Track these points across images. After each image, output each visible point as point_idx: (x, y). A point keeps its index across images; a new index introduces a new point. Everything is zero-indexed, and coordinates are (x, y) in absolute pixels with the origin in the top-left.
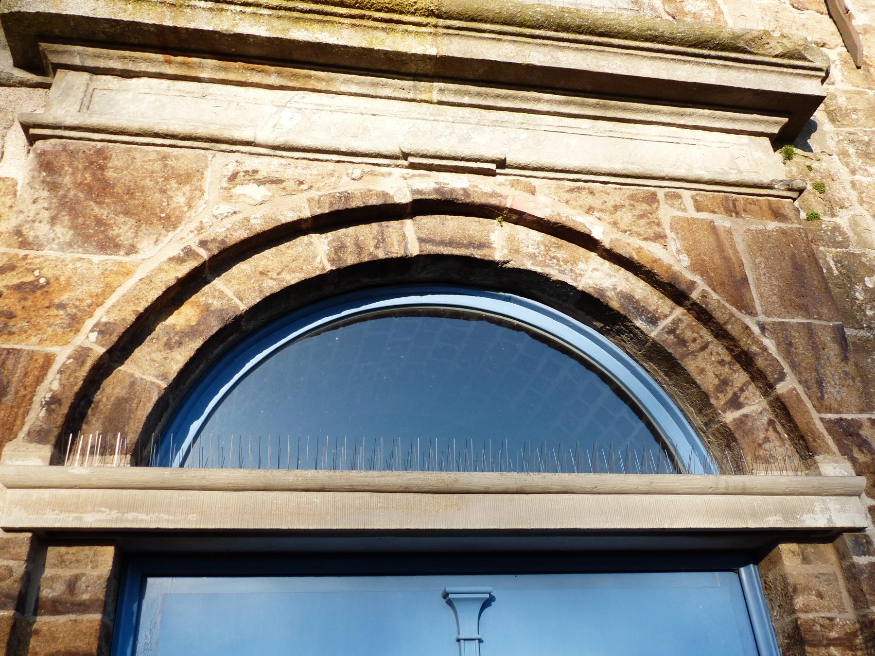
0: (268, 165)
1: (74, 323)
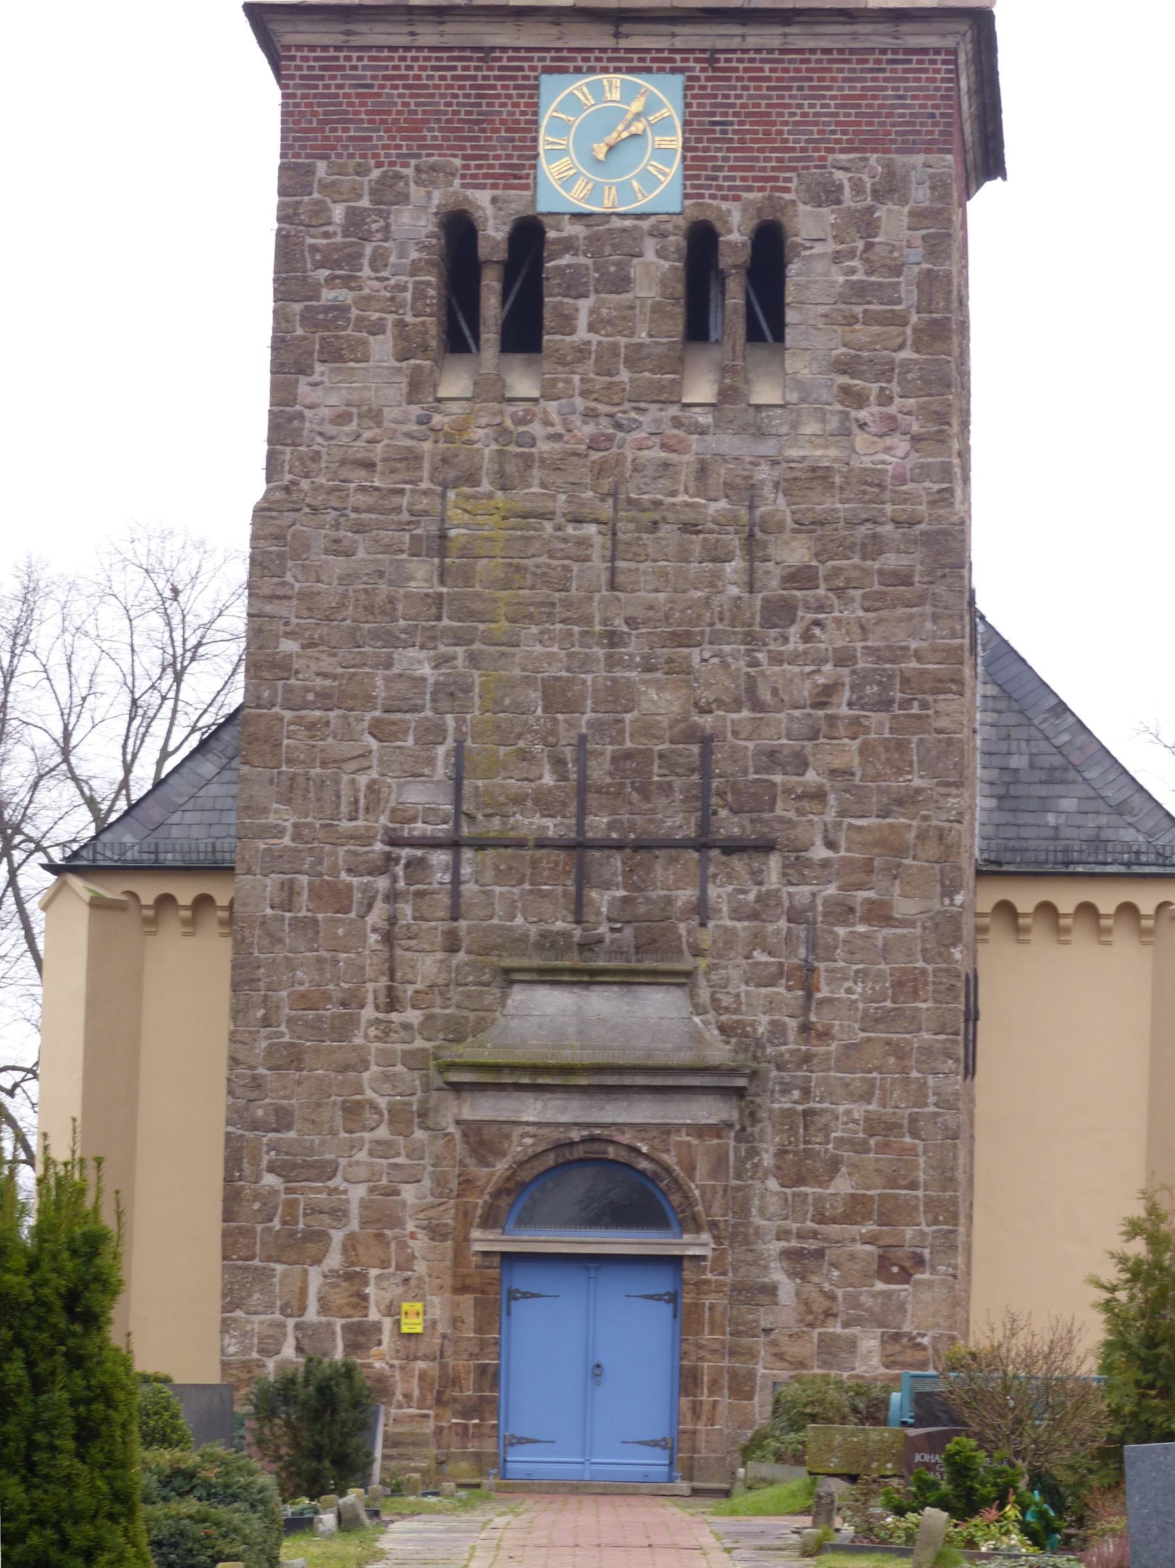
0: (531, 1130)
1: (482, 1192)
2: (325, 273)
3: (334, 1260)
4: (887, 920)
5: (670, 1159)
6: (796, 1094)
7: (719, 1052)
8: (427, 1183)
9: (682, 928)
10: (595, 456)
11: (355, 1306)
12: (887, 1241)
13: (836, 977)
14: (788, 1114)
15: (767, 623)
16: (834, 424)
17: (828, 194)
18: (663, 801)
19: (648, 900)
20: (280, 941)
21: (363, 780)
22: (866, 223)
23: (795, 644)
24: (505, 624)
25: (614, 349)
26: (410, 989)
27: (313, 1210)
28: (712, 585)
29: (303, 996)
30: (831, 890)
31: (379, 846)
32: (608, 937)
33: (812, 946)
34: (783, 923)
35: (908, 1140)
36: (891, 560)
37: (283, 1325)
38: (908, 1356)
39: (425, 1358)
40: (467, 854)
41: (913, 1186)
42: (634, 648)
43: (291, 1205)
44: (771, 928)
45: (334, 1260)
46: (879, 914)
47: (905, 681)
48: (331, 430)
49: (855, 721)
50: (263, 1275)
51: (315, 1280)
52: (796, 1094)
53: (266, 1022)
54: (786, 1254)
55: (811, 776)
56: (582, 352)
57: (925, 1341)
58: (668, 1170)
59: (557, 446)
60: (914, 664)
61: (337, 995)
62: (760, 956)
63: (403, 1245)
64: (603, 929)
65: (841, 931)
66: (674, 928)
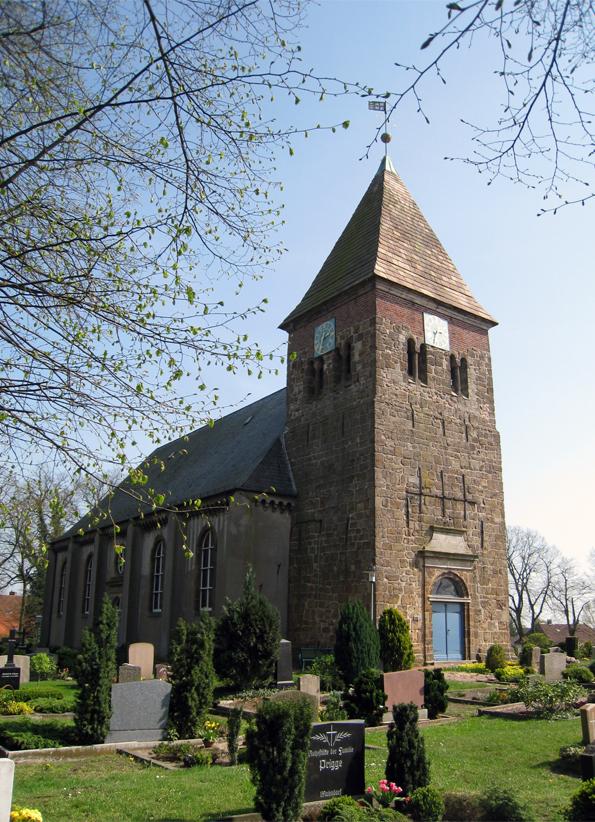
3: (399, 602)
17: (473, 356)
45: (399, 602)
54: (482, 602)
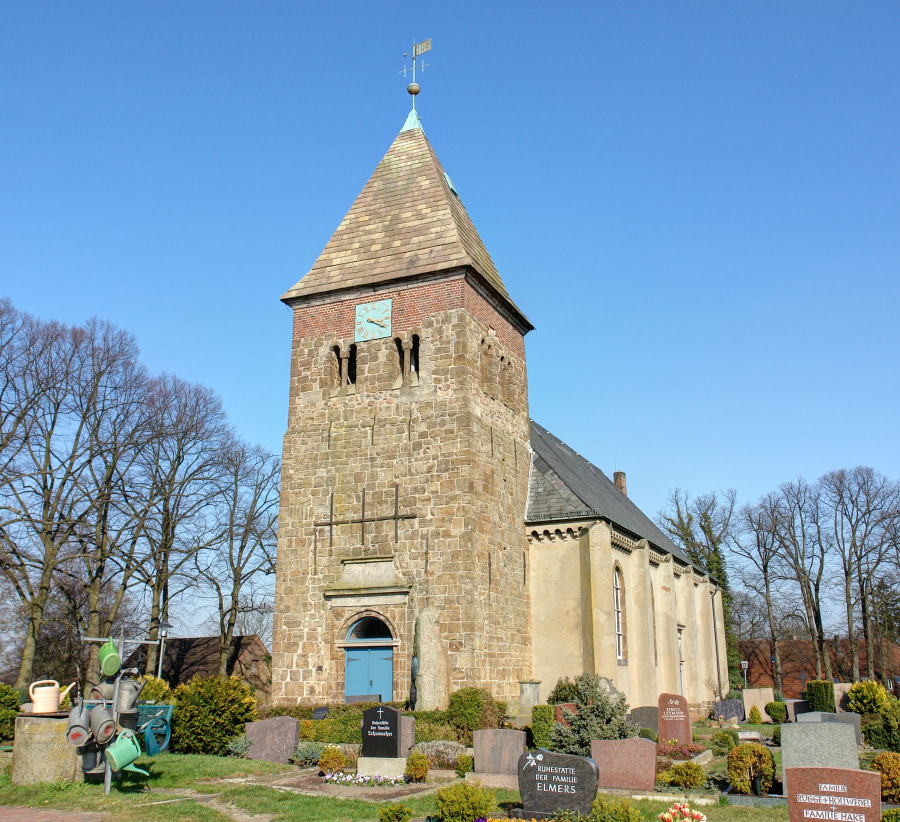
2: (302, 368)
3: (300, 651)
4: (449, 536)
5: (388, 615)
6: (424, 593)
7: (404, 580)
8: (324, 626)
9: (391, 544)
10: (370, 408)
11: (305, 665)
12: (451, 638)
13: (435, 555)
14: (422, 599)
15: (414, 450)
16: (432, 389)
17: (430, 324)
18: (385, 506)
19: (382, 536)
20: (288, 556)
21: (309, 508)
22: (440, 331)
23: (422, 455)
24: (345, 458)
25: (374, 377)
26: (320, 568)
27: (295, 636)
28: (399, 440)
29: (294, 572)
30: (433, 528)
31: (313, 527)
32: (371, 548)
33: (427, 547)
34: (419, 540)
35: (457, 605)
36: (447, 427)
37: (287, 671)
38: (459, 675)
39: (324, 680)
40: (334, 526)
41: (458, 620)
42: (379, 461)
43: (290, 634)
44: (416, 541)
45: (300, 651)
46: (447, 534)
47: (452, 462)
48: (303, 410)
49: (439, 476)
50: (283, 656)
51: (295, 658)
52: (424, 593)
53: (284, 581)
55: (426, 494)
56: (366, 379)
57: (464, 670)
58: (387, 619)
59: (360, 406)
60: (455, 457)
61: (301, 572)
62: (413, 550)
63: (318, 646)
64: (370, 545)
65: (436, 541)
66: (389, 544)
